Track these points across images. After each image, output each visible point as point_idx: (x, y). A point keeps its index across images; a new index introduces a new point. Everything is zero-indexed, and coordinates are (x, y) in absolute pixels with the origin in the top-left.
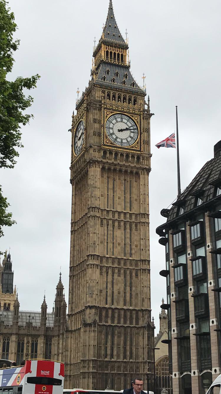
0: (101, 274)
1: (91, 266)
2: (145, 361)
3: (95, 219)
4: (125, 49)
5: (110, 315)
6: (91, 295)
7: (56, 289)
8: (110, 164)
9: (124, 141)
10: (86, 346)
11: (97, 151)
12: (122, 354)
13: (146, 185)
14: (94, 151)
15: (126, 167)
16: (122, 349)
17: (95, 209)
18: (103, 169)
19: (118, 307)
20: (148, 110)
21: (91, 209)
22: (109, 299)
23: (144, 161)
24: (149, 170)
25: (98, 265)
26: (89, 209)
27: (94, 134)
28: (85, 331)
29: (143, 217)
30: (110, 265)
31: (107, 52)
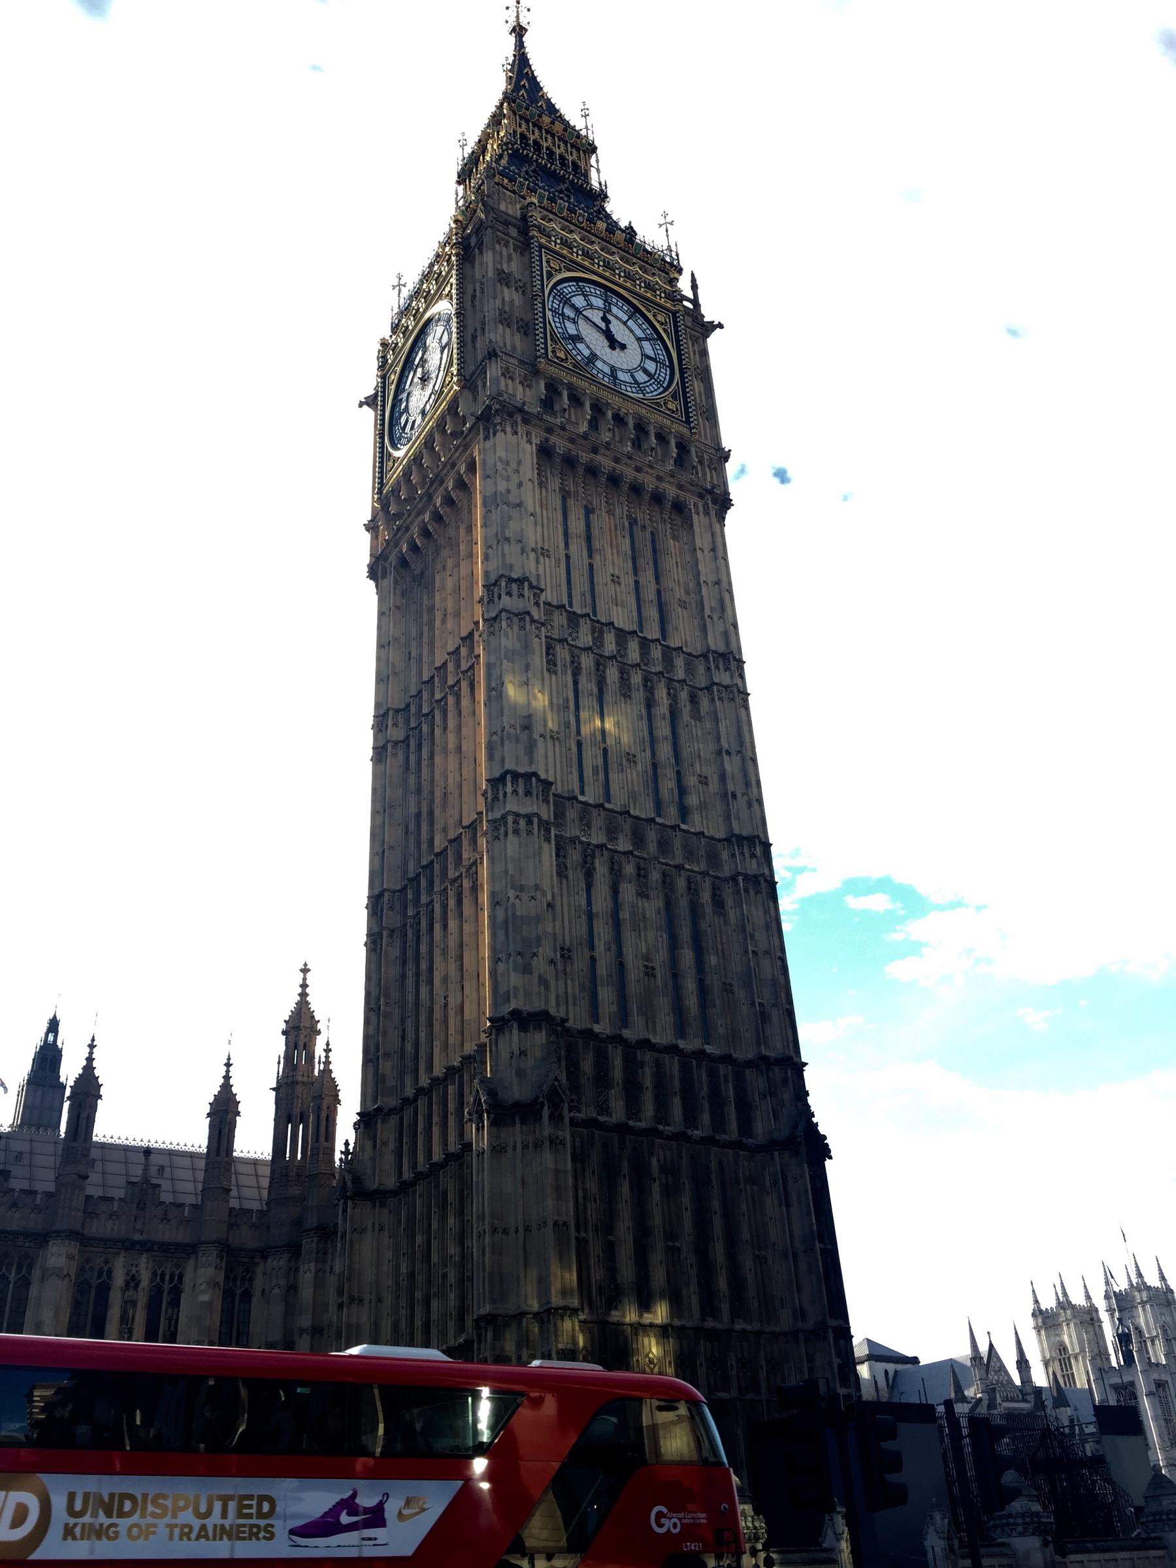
0: (562, 873)
1: (516, 822)
4: (584, 152)
5: (617, 1073)
7: (284, 1033)
10: (505, 1232)
12: (694, 1287)
14: (503, 374)
15: (638, 469)
17: (520, 587)
18: (545, 452)
21: (503, 584)
22: (606, 994)
23: (703, 470)
24: (724, 503)
27: (505, 319)
28: (497, 1149)
30: (597, 837)
31: (523, 136)
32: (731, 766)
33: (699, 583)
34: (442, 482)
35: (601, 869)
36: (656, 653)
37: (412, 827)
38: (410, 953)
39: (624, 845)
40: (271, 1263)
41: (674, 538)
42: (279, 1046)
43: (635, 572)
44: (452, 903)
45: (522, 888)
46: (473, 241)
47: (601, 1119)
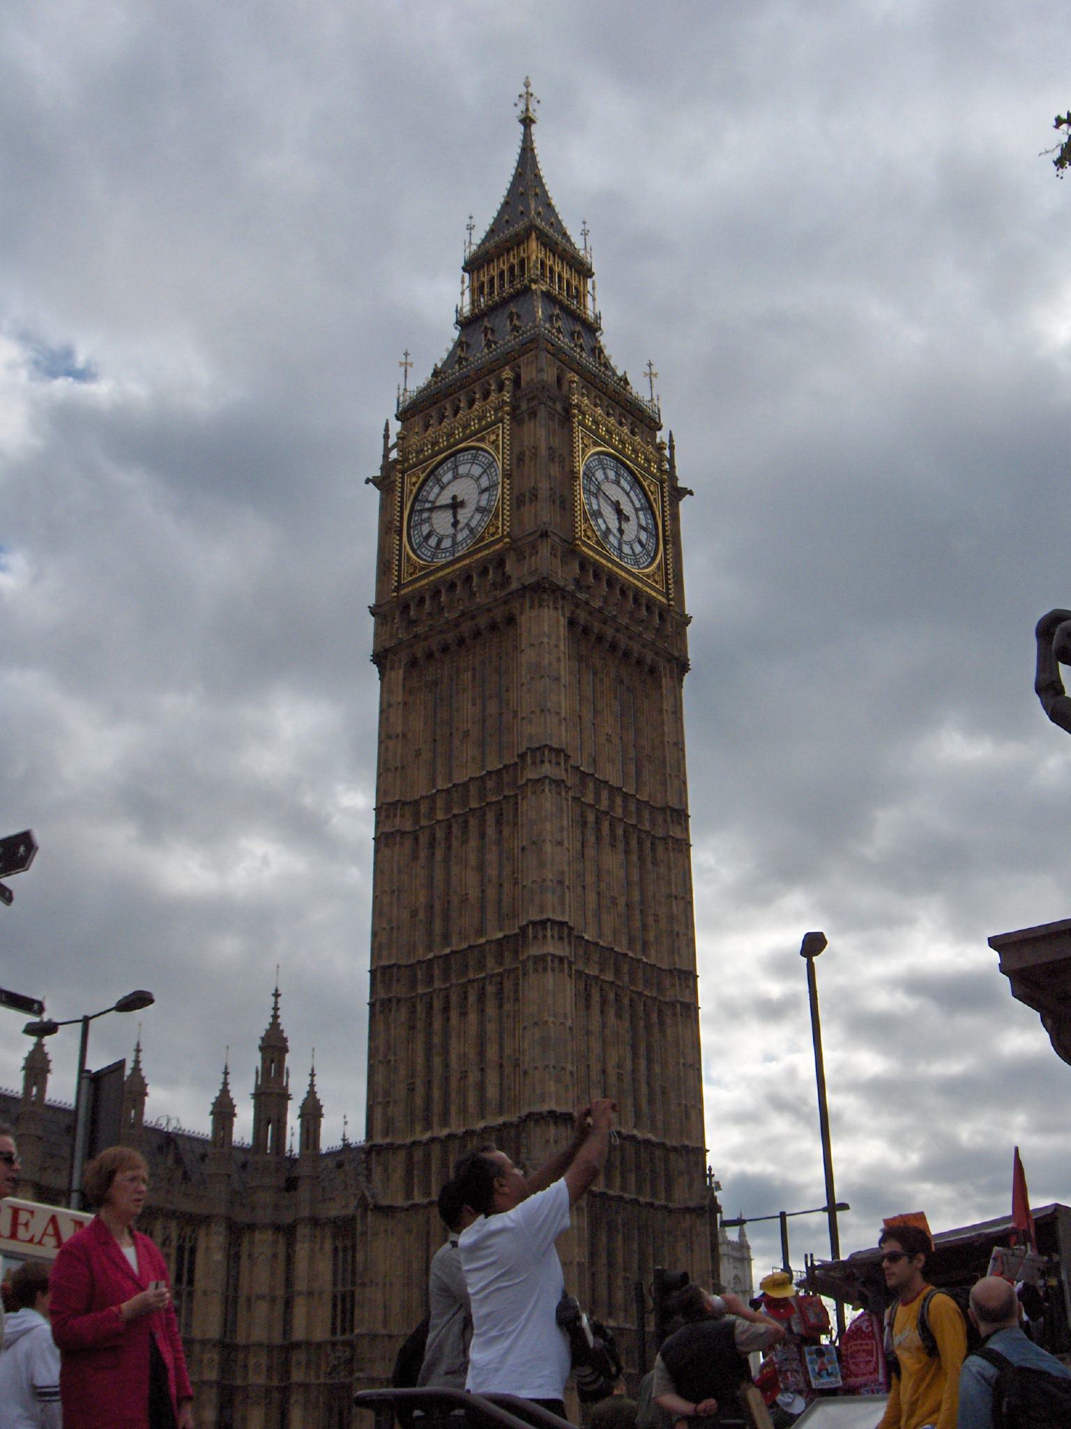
3: (559, 794)
9: (626, 549)
11: (559, 554)
15: (630, 638)
18: (572, 623)
24: (683, 667)
26: (534, 751)
30: (593, 971)
31: (542, 263)
32: (677, 909)
33: (662, 742)
34: (473, 618)
35: (596, 997)
37: (421, 915)
38: (420, 1025)
39: (609, 977)
40: (258, 1236)
42: (256, 1059)
44: (472, 998)
46: (524, 406)
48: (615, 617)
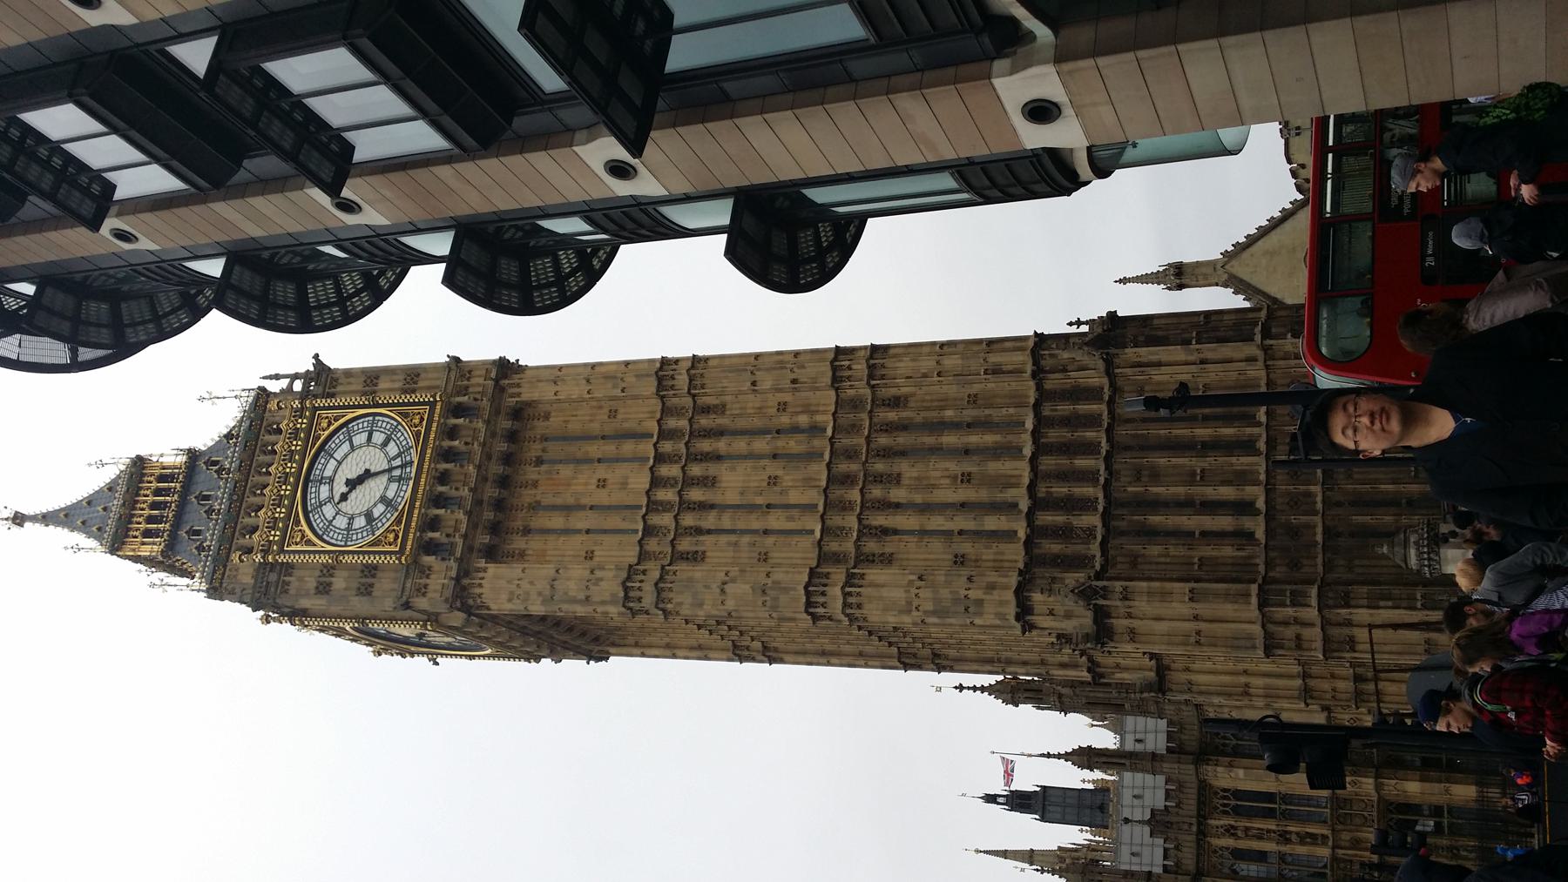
0: (887, 560)
2: (1259, 353)
3: (670, 589)
5: (1060, 519)
6: (971, 607)
8: (473, 525)
12: (1234, 460)
13: (558, 374)
16: (1208, 462)
18: (492, 554)
19: (1026, 481)
20: (306, 377)
25: (850, 576)
26: (634, 613)
27: (366, 591)
29: (671, 383)
30: (852, 521)
36: (667, 447)
39: (855, 495)
41: (547, 417)
43: (588, 461)
45: (909, 603)
47: (1099, 538)
48: (471, 490)
